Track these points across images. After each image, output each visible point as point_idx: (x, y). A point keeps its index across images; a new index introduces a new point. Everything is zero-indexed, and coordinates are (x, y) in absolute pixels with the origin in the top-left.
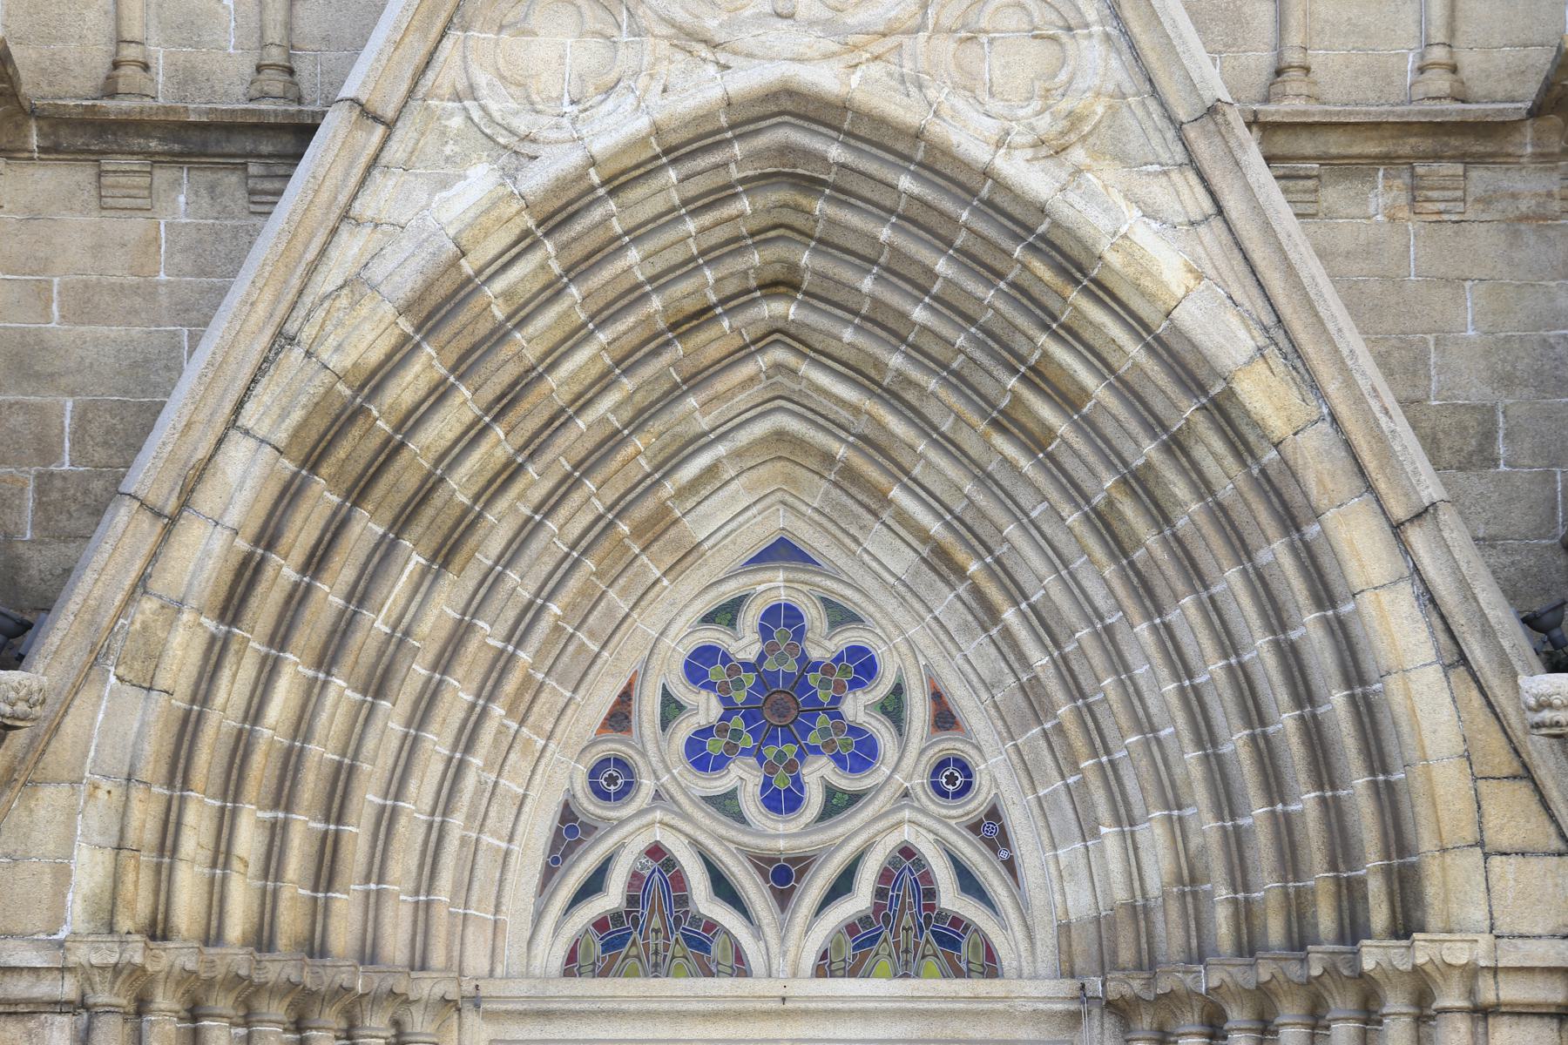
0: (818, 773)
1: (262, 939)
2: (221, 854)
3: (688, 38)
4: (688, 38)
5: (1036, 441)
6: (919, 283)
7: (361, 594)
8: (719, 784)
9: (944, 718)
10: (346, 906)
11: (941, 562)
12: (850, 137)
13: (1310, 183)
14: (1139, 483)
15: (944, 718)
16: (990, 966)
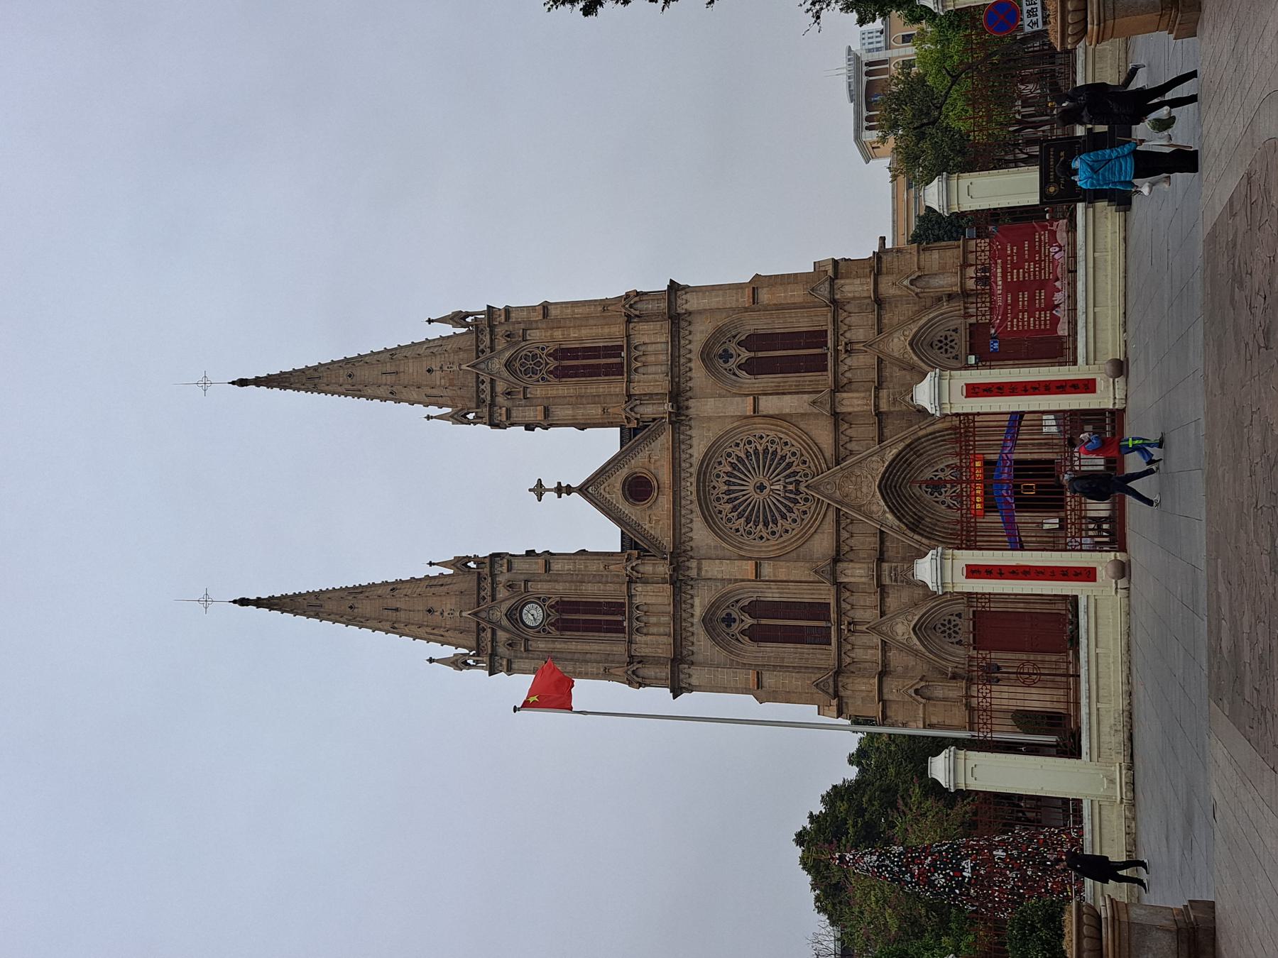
3: (873, 496)
4: (873, 496)
6: (896, 474)
7: (928, 527)
8: (943, 492)
9: (937, 471)
11: (921, 471)
12: (883, 480)
15: (937, 471)
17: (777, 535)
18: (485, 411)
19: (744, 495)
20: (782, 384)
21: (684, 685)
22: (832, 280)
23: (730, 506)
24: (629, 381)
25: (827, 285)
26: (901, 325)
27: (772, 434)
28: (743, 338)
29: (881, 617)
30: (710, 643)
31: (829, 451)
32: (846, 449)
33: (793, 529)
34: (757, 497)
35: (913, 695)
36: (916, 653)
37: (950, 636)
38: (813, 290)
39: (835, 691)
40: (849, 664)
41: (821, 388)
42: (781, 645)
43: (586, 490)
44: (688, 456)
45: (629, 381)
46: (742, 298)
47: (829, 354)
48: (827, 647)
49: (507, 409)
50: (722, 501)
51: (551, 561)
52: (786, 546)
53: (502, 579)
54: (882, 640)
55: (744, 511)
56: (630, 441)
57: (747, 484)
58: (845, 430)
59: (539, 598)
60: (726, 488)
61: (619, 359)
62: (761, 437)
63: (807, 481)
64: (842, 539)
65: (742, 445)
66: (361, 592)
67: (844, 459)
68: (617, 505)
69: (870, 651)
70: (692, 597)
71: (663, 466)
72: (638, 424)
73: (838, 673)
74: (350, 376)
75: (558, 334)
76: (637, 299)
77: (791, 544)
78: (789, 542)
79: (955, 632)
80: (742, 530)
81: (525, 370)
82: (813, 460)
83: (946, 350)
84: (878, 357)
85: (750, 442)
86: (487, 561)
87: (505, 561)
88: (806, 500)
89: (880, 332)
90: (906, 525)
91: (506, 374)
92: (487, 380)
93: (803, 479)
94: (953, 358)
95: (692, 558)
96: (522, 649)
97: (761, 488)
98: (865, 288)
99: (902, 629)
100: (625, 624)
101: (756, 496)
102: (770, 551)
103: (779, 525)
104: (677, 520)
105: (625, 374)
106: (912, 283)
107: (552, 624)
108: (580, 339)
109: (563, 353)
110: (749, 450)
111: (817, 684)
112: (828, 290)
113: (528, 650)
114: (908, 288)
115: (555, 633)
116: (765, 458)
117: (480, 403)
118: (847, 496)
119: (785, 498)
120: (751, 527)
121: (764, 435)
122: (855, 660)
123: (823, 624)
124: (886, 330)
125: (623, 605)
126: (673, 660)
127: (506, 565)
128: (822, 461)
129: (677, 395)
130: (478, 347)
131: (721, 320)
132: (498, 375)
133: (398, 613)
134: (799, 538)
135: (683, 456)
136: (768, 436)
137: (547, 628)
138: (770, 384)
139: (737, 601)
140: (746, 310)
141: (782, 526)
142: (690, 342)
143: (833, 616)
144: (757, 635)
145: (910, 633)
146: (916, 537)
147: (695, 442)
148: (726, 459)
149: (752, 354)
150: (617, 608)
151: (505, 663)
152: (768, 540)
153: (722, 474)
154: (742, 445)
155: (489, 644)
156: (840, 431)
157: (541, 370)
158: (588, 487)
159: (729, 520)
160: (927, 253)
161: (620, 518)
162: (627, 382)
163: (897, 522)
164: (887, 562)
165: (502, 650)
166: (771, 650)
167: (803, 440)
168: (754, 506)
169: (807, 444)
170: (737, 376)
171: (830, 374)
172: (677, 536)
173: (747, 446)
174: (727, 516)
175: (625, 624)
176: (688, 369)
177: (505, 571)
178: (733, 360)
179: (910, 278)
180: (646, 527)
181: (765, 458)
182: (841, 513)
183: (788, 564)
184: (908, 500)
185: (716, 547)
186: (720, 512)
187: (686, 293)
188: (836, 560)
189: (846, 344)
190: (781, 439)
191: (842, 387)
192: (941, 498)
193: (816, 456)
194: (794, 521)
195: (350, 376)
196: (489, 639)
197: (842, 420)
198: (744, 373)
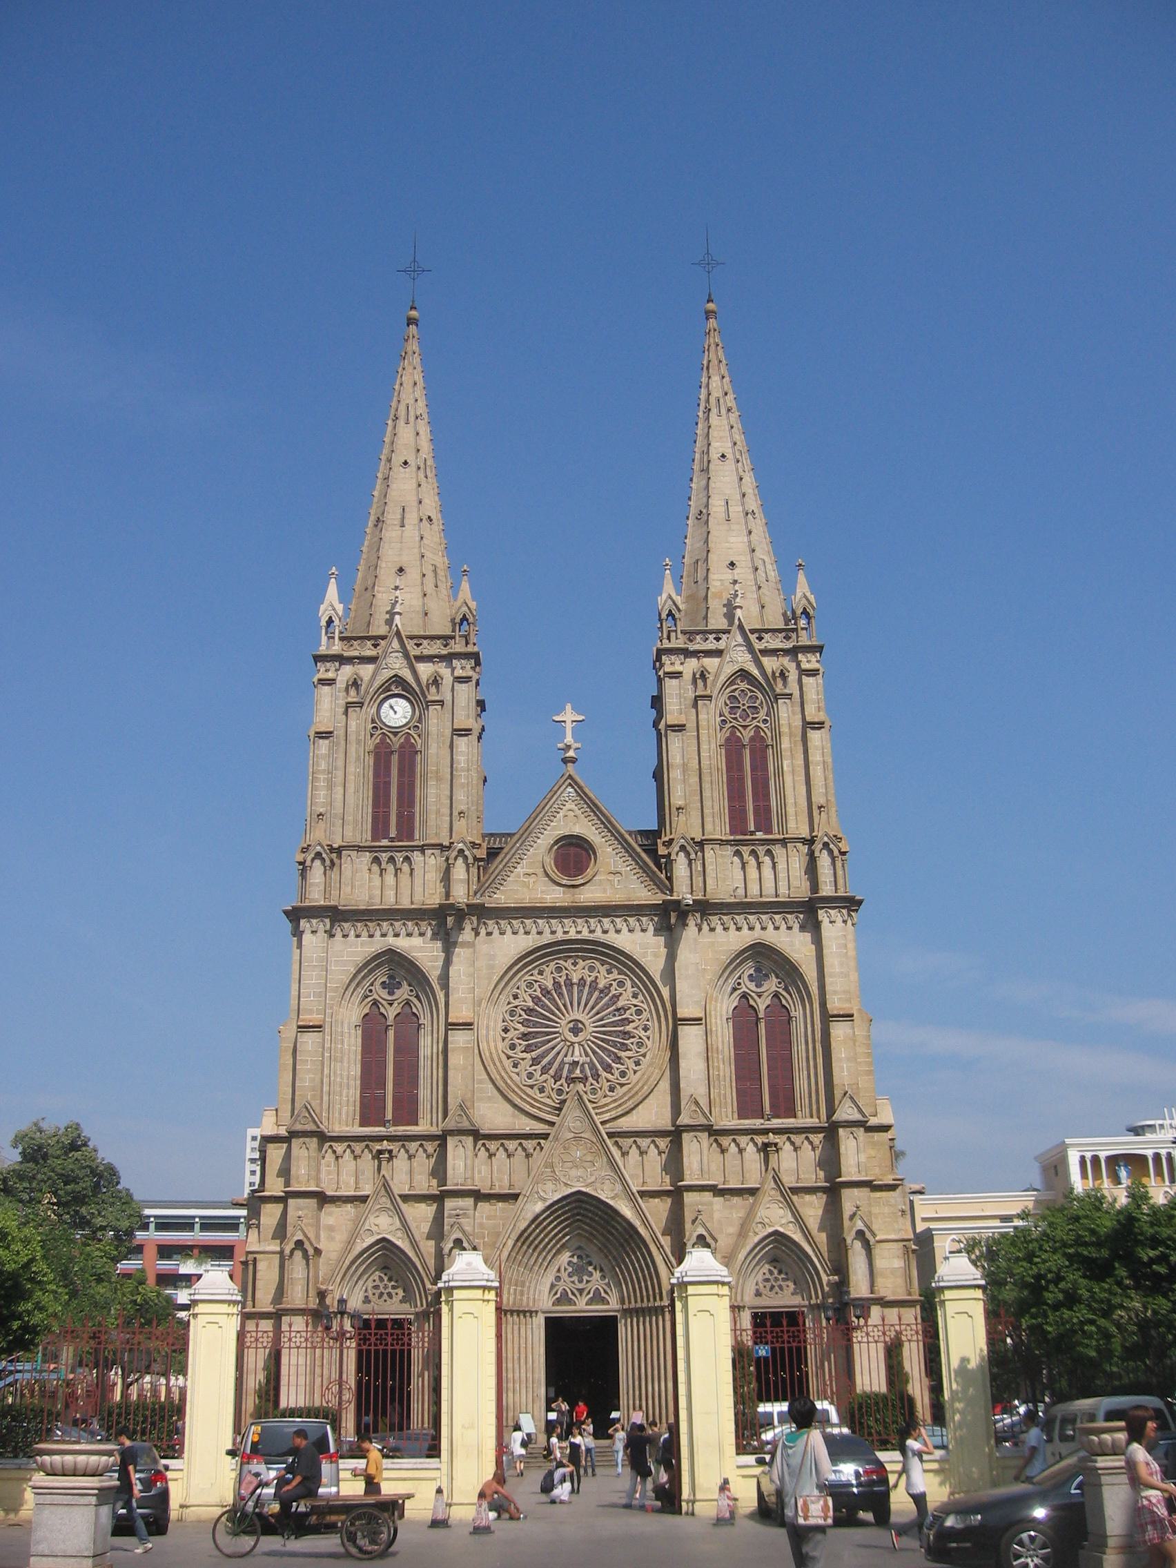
0: (585, 1278)
1: (514, 1303)
2: (509, 1293)
3: (566, 1184)
4: (566, 1184)
5: (612, 1234)
10: (525, 1298)
14: (626, 1240)
16: (608, 1303)
17: (510, 1053)
18: (678, 642)
19: (565, 1006)
20: (721, 1057)
21: (303, 923)
22: (861, 1124)
23: (550, 987)
24: (722, 843)
25: (857, 1117)
26: (799, 1220)
27: (649, 1043)
28: (784, 1002)
29: (400, 1196)
30: (360, 959)
31: (625, 1124)
32: (631, 1147)
33: (518, 1074)
34: (563, 1026)
35: (296, 1238)
36: (350, 1242)
37: (376, 1287)
38: (851, 1098)
39: (298, 1132)
40: (334, 1152)
41: (715, 1111)
42: (359, 1057)
43: (570, 785)
44: (619, 926)
45: (722, 843)
46: (840, 999)
47: (762, 1121)
48: (357, 1121)
49: (681, 673)
50: (556, 975)
52: (495, 1064)
53: (444, 671)
54: (368, 1196)
55: (544, 1007)
56: (640, 845)
57: (581, 1008)
58: (657, 1147)
59: (420, 721)
60: (575, 980)
61: (753, 829)
62: (646, 1029)
63: (586, 1093)
65: (635, 1002)
66: (426, 477)
67: (616, 1143)
68: (549, 828)
69: (352, 1180)
70: (422, 935)
71: (605, 891)
72: (663, 856)
73: (323, 1138)
74: (723, 456)
75: (786, 743)
76: (836, 853)
77: (498, 1071)
78: (500, 1068)
79: (381, 1294)
80: (516, 1003)
81: (735, 697)
82: (615, 1101)
83: (767, 1280)
84: (758, 1189)
86: (470, 649)
87: (471, 673)
88: (560, 1092)
89: (795, 1190)
90: (525, 1230)
91: (729, 670)
92: (722, 645)
93: (589, 1088)
94: (757, 1290)
95: (477, 934)
96: (350, 700)
97: (576, 1031)
98: (854, 1170)
99: (383, 1225)
100: (385, 842)
101: (563, 1023)
102: (488, 1042)
103: (524, 1055)
105: (732, 838)
106: (860, 1234)
107: (383, 741)
108: (780, 773)
109: (760, 748)
111: (307, 1108)
112: (851, 1118)
113: (347, 708)
114: (852, 1227)
115: (371, 744)
116: (616, 1034)
117: (690, 635)
118: (565, 1148)
119: (562, 1063)
120: (520, 1016)
121: (648, 1033)
122: (340, 1160)
123: (389, 1116)
124: (795, 1198)
125: (411, 838)
126: (334, 909)
127: (464, 675)
128: (613, 1114)
129: (705, 908)
130: (767, 631)
131: (810, 973)
132: (728, 659)
133: (398, 528)
134: (506, 1083)
135: (618, 920)
136: (648, 1038)
137: (379, 732)
138: (720, 1039)
140: (823, 1004)
141: (523, 1059)
142: (777, 928)
143: (401, 1130)
144: (372, 1028)
145: (379, 1234)
146: (510, 1243)
147: (638, 934)
148: (615, 980)
149: (761, 1015)
150: (407, 828)
151: (330, 675)
152: (504, 1039)
153: (594, 974)
154: (635, 1002)
155: (356, 653)
157: (735, 719)
158: (573, 787)
159: (530, 985)
160: (900, 1252)
162: (721, 840)
163: (530, 1217)
164: (476, 1205)
165: (347, 671)
166: (351, 1044)
167: (642, 1087)
168: (550, 1020)
169: (637, 1093)
170: (732, 993)
171: (732, 1122)
174: (536, 981)
175: (385, 842)
176: (739, 926)
177: (456, 674)
178: (754, 988)
179: (865, 1229)
180: (519, 869)
181: (616, 1034)
182: (542, 1141)
183: (470, 1068)
184: (559, 1232)
185: (491, 967)
186: (541, 973)
187: (845, 922)
188: (476, 1135)
189: (776, 1145)
191: (716, 1141)
192: (564, 1275)
193: (620, 1105)
194: (530, 1076)
195: (723, 456)
196: (363, 654)
197: (671, 1141)
198: (735, 1004)
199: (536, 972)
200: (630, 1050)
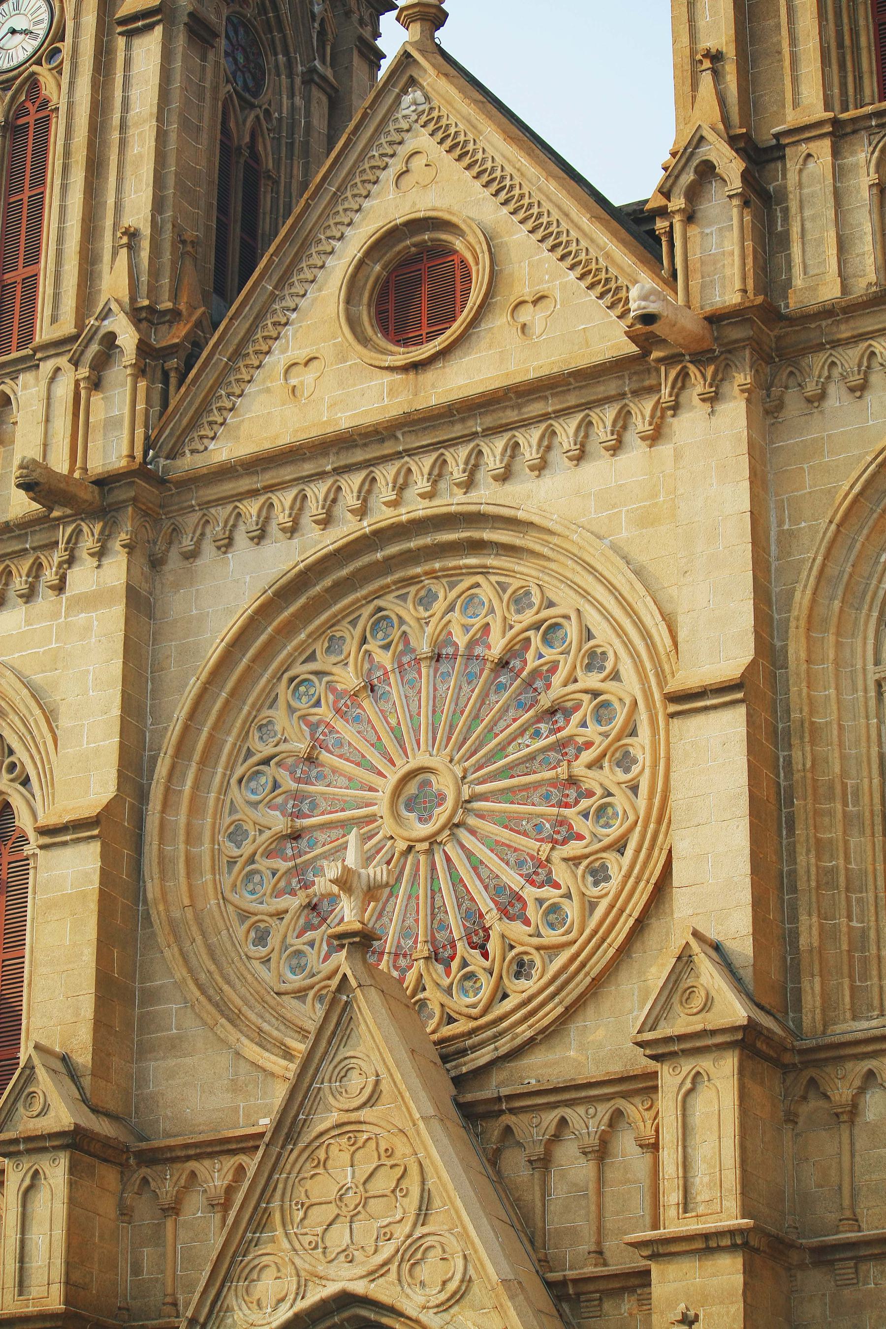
13: (596, 1303)
43: (412, 82)
51: (159, 30)
64: (202, 1168)
65: (592, 681)
85: (603, 712)
95: (156, 563)
104: (287, 473)
110: (576, 718)
120: (276, 785)
121: (635, 769)
139: (26, 782)
141: (280, 915)
148: (536, 626)
154: (592, 681)
156: (621, 1103)
161: (305, 245)
172: (228, 488)
173: (588, 705)
190: (621, 851)
199: (320, 647)
200: (580, 837)
